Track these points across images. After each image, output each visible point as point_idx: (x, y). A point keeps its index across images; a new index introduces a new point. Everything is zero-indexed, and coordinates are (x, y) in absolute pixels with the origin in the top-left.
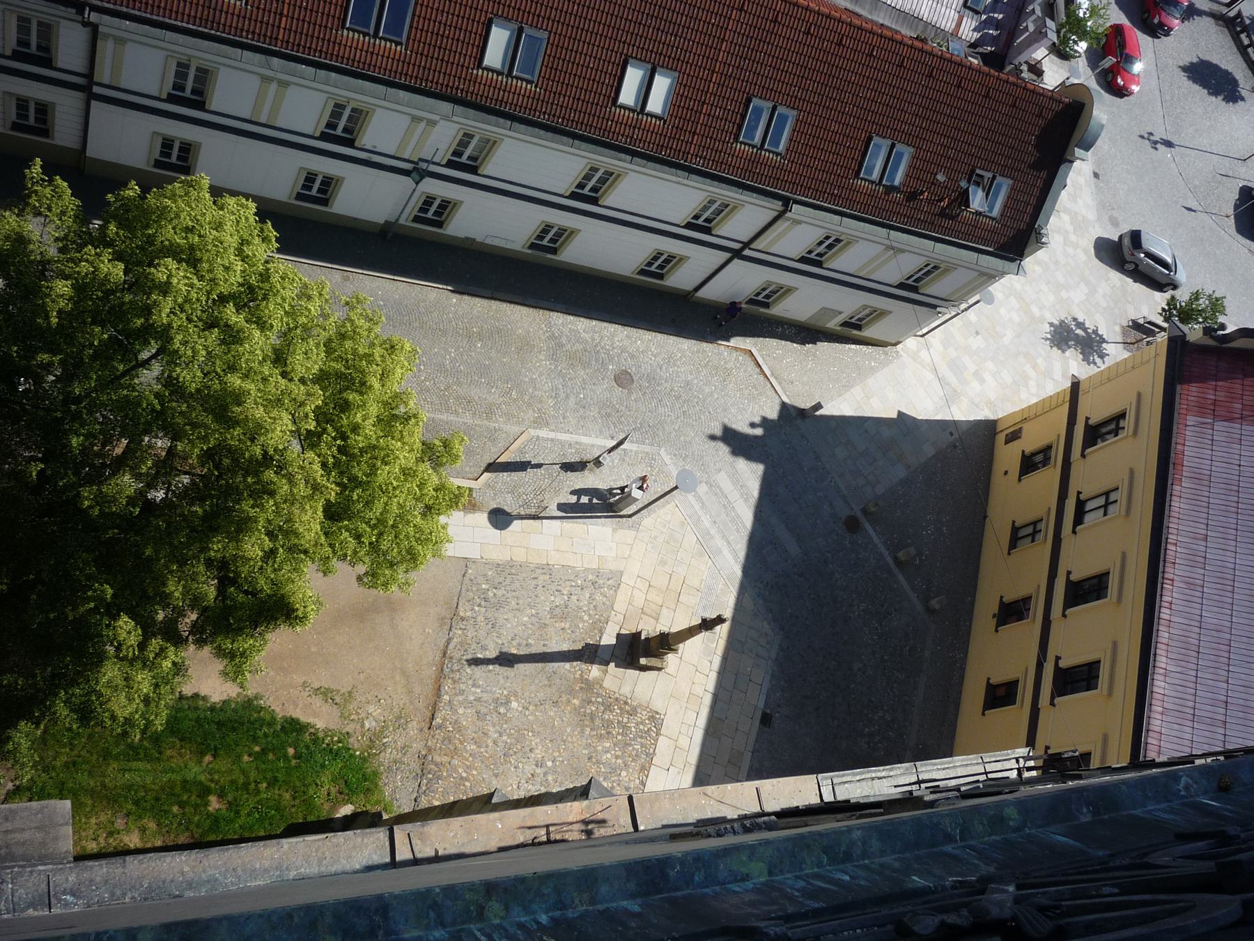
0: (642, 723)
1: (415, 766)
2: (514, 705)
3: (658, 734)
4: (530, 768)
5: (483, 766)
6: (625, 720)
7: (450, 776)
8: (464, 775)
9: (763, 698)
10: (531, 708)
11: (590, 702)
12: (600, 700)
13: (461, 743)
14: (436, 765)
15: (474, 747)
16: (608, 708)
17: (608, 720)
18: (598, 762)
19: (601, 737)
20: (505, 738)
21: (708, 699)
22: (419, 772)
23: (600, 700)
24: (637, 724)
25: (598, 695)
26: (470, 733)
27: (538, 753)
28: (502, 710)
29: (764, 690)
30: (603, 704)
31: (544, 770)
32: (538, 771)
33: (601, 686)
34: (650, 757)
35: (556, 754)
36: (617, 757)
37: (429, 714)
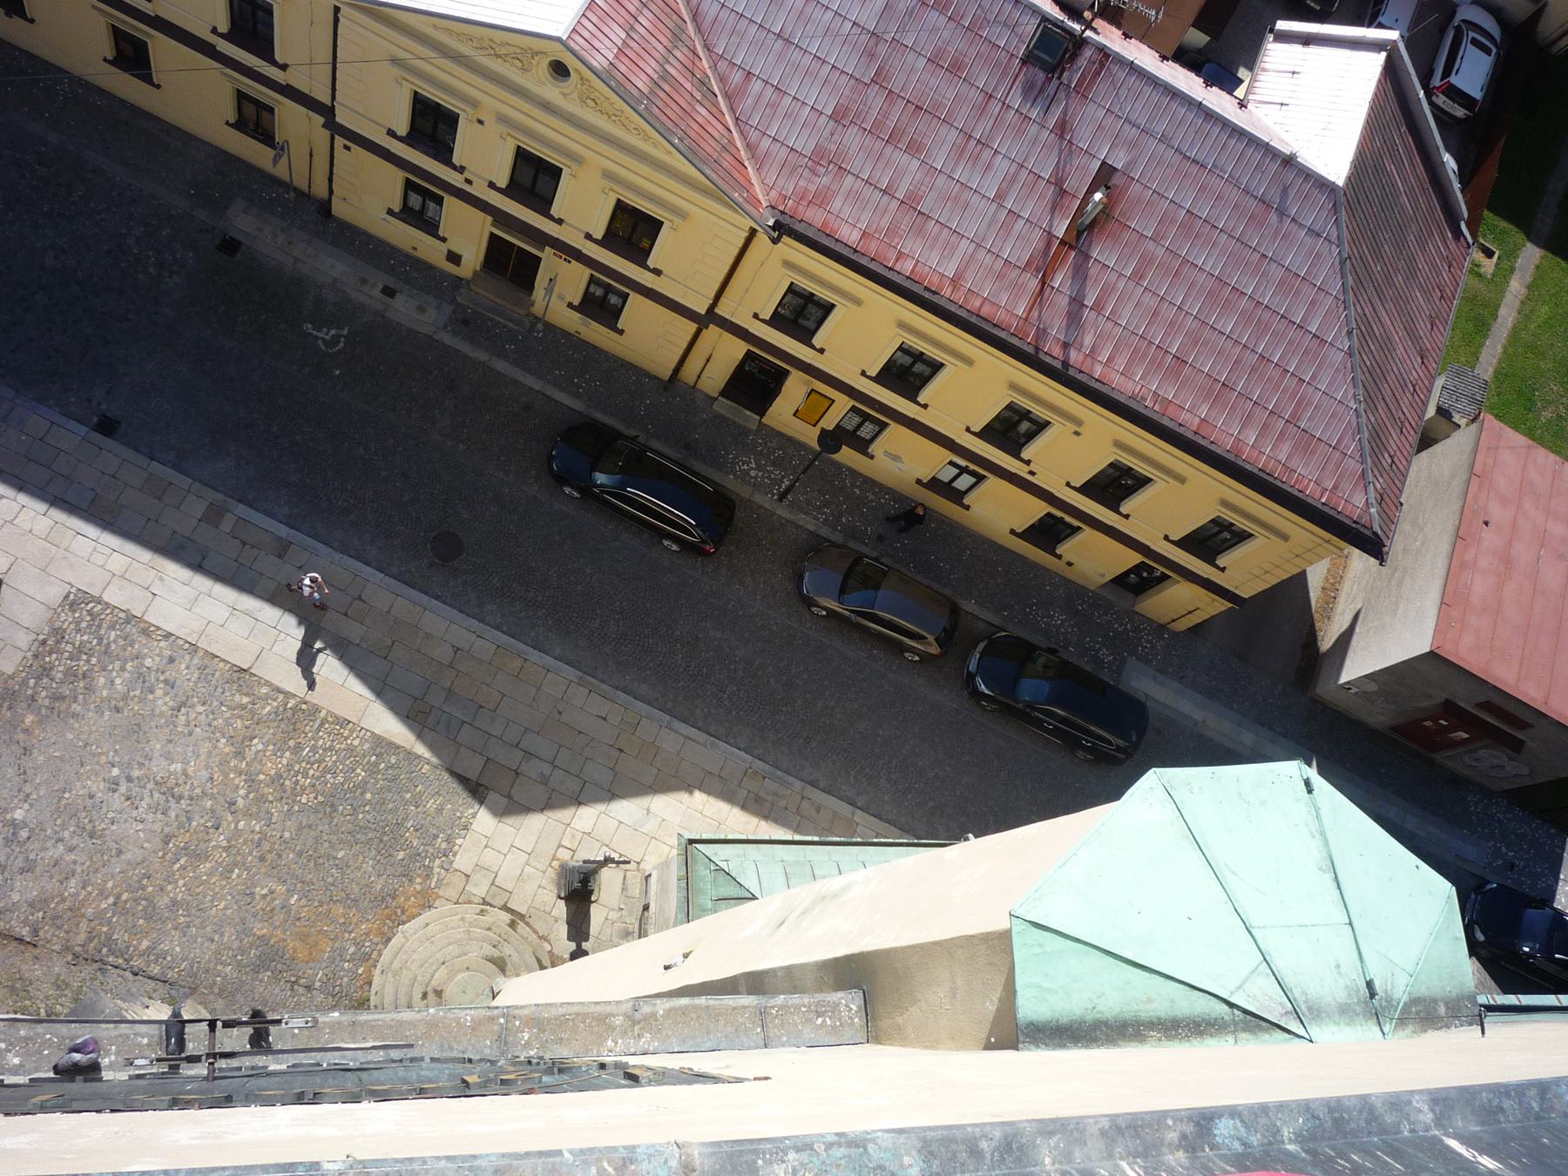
0: (78, 623)
1: (88, 970)
2: (18, 815)
3: (99, 601)
4: (117, 801)
5: (104, 870)
6: (69, 648)
7: (109, 922)
8: (111, 900)
9: (73, 425)
10: (28, 789)
11: (33, 698)
12: (32, 682)
13: (64, 900)
14: (91, 939)
15: (72, 883)
16: (47, 671)
17: (66, 673)
18: (125, 698)
19: (89, 689)
20: (66, 834)
21: (57, 515)
22: (96, 966)
23: (32, 682)
24: (78, 630)
25: (24, 683)
26: (51, 886)
27: (97, 786)
28: (24, 834)
29: (61, 420)
30: (39, 678)
31: (123, 782)
32: (123, 789)
33: (12, 677)
34: (130, 618)
35: (103, 759)
36: (123, 669)
37: (14, 943)
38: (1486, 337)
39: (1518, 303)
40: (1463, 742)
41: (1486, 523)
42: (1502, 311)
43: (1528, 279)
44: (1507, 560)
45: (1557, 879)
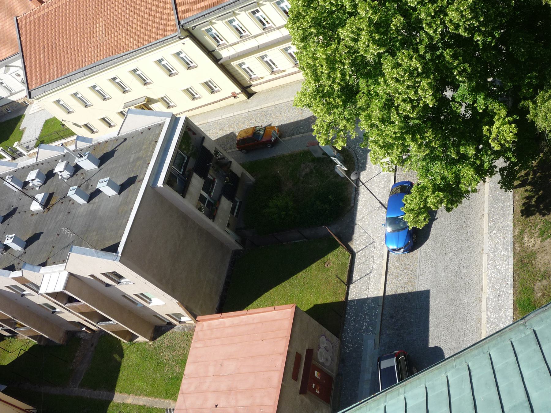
38: (153, 408)
39: (137, 397)
40: (320, 370)
41: (216, 406)
42: (141, 403)
43: (126, 395)
44: (230, 391)
45: (368, 299)
